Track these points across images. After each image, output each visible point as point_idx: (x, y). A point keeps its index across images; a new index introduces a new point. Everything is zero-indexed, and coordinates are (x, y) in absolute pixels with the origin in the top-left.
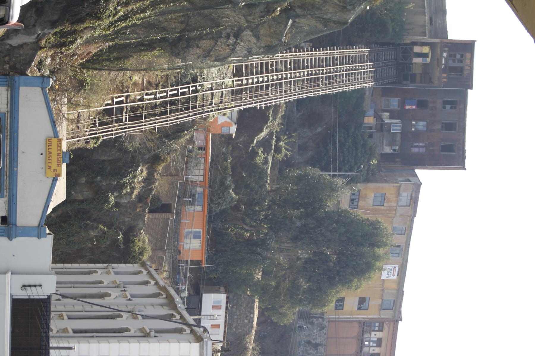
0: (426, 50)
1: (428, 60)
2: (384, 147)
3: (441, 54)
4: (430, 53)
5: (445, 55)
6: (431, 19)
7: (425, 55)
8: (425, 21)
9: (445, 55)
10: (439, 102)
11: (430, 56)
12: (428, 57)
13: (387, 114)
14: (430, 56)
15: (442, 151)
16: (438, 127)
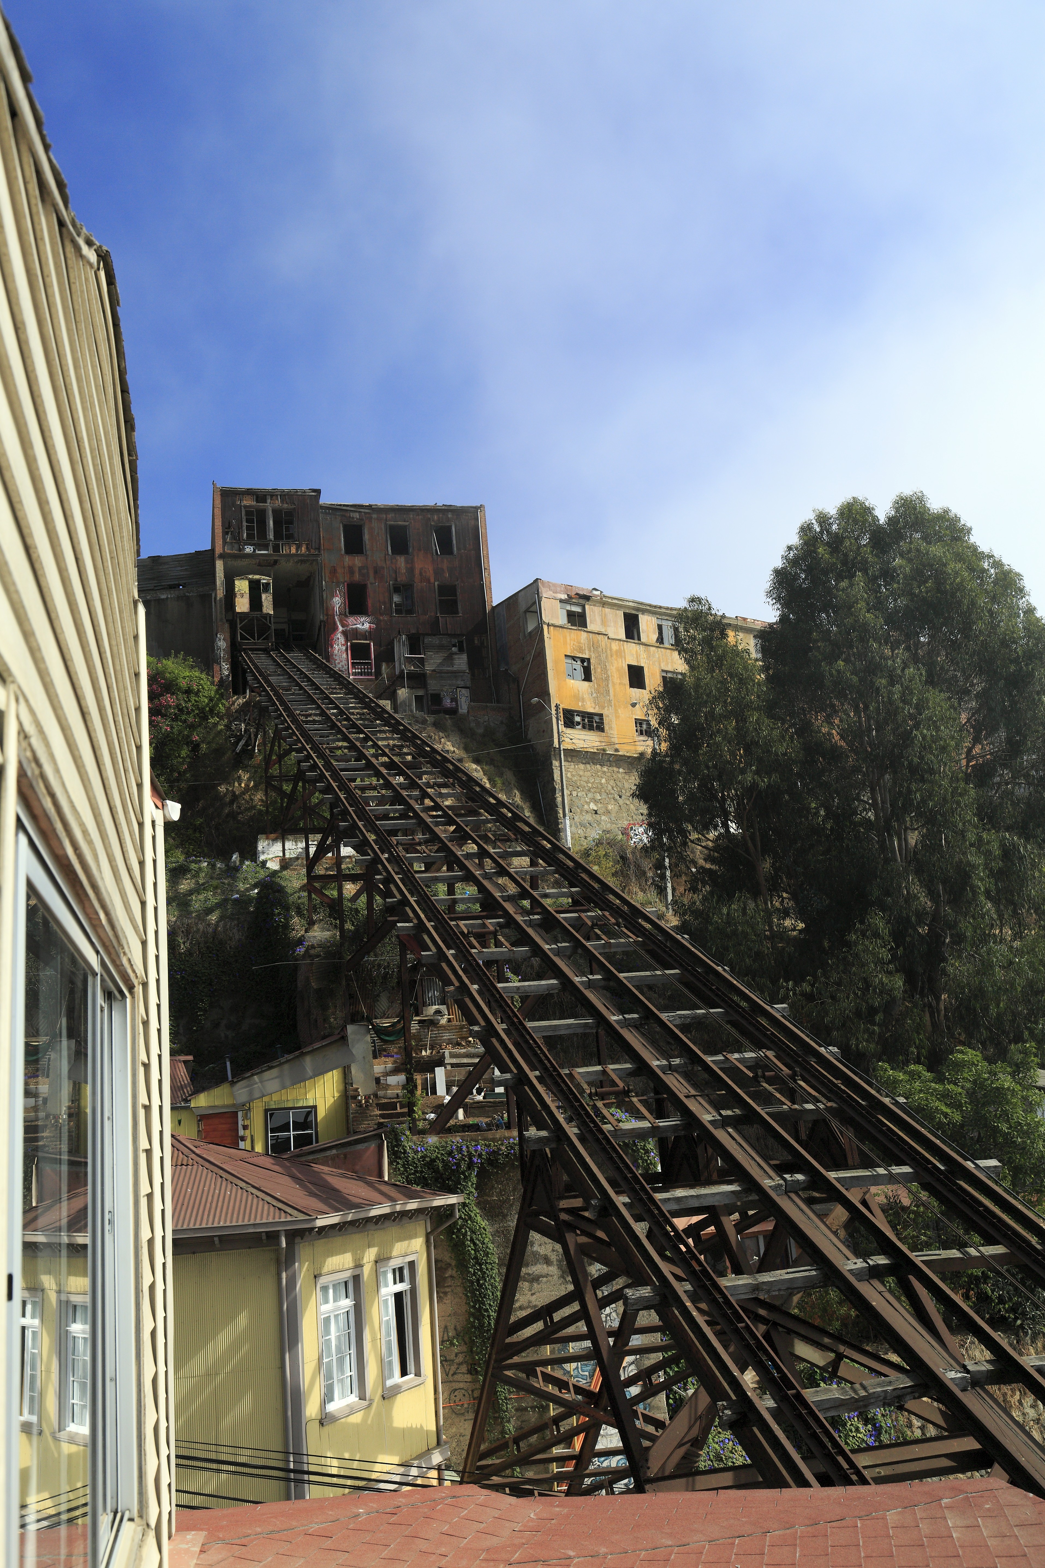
0: (242, 586)
1: (264, 580)
2: (455, 668)
3: (248, 556)
4: (250, 577)
5: (249, 549)
6: (172, 587)
7: (255, 589)
8: (178, 598)
9: (249, 549)
10: (347, 559)
11: (257, 577)
12: (258, 582)
13: (384, 667)
14: (257, 577)
15: (451, 552)
16: (401, 561)
